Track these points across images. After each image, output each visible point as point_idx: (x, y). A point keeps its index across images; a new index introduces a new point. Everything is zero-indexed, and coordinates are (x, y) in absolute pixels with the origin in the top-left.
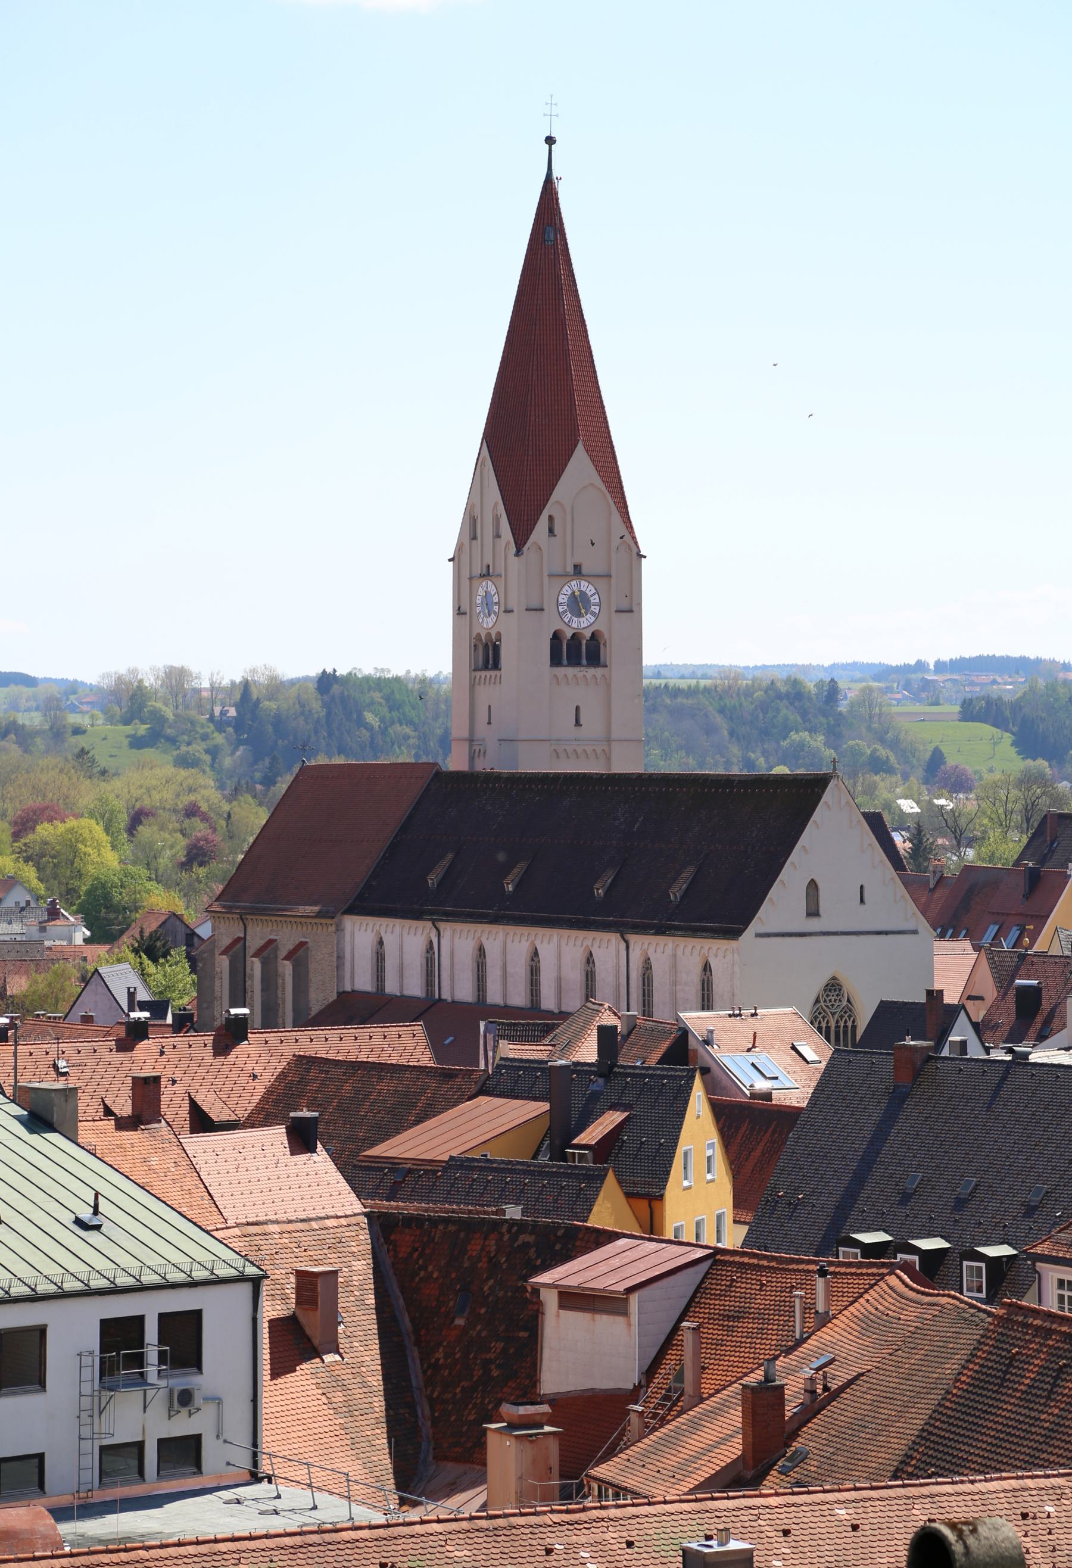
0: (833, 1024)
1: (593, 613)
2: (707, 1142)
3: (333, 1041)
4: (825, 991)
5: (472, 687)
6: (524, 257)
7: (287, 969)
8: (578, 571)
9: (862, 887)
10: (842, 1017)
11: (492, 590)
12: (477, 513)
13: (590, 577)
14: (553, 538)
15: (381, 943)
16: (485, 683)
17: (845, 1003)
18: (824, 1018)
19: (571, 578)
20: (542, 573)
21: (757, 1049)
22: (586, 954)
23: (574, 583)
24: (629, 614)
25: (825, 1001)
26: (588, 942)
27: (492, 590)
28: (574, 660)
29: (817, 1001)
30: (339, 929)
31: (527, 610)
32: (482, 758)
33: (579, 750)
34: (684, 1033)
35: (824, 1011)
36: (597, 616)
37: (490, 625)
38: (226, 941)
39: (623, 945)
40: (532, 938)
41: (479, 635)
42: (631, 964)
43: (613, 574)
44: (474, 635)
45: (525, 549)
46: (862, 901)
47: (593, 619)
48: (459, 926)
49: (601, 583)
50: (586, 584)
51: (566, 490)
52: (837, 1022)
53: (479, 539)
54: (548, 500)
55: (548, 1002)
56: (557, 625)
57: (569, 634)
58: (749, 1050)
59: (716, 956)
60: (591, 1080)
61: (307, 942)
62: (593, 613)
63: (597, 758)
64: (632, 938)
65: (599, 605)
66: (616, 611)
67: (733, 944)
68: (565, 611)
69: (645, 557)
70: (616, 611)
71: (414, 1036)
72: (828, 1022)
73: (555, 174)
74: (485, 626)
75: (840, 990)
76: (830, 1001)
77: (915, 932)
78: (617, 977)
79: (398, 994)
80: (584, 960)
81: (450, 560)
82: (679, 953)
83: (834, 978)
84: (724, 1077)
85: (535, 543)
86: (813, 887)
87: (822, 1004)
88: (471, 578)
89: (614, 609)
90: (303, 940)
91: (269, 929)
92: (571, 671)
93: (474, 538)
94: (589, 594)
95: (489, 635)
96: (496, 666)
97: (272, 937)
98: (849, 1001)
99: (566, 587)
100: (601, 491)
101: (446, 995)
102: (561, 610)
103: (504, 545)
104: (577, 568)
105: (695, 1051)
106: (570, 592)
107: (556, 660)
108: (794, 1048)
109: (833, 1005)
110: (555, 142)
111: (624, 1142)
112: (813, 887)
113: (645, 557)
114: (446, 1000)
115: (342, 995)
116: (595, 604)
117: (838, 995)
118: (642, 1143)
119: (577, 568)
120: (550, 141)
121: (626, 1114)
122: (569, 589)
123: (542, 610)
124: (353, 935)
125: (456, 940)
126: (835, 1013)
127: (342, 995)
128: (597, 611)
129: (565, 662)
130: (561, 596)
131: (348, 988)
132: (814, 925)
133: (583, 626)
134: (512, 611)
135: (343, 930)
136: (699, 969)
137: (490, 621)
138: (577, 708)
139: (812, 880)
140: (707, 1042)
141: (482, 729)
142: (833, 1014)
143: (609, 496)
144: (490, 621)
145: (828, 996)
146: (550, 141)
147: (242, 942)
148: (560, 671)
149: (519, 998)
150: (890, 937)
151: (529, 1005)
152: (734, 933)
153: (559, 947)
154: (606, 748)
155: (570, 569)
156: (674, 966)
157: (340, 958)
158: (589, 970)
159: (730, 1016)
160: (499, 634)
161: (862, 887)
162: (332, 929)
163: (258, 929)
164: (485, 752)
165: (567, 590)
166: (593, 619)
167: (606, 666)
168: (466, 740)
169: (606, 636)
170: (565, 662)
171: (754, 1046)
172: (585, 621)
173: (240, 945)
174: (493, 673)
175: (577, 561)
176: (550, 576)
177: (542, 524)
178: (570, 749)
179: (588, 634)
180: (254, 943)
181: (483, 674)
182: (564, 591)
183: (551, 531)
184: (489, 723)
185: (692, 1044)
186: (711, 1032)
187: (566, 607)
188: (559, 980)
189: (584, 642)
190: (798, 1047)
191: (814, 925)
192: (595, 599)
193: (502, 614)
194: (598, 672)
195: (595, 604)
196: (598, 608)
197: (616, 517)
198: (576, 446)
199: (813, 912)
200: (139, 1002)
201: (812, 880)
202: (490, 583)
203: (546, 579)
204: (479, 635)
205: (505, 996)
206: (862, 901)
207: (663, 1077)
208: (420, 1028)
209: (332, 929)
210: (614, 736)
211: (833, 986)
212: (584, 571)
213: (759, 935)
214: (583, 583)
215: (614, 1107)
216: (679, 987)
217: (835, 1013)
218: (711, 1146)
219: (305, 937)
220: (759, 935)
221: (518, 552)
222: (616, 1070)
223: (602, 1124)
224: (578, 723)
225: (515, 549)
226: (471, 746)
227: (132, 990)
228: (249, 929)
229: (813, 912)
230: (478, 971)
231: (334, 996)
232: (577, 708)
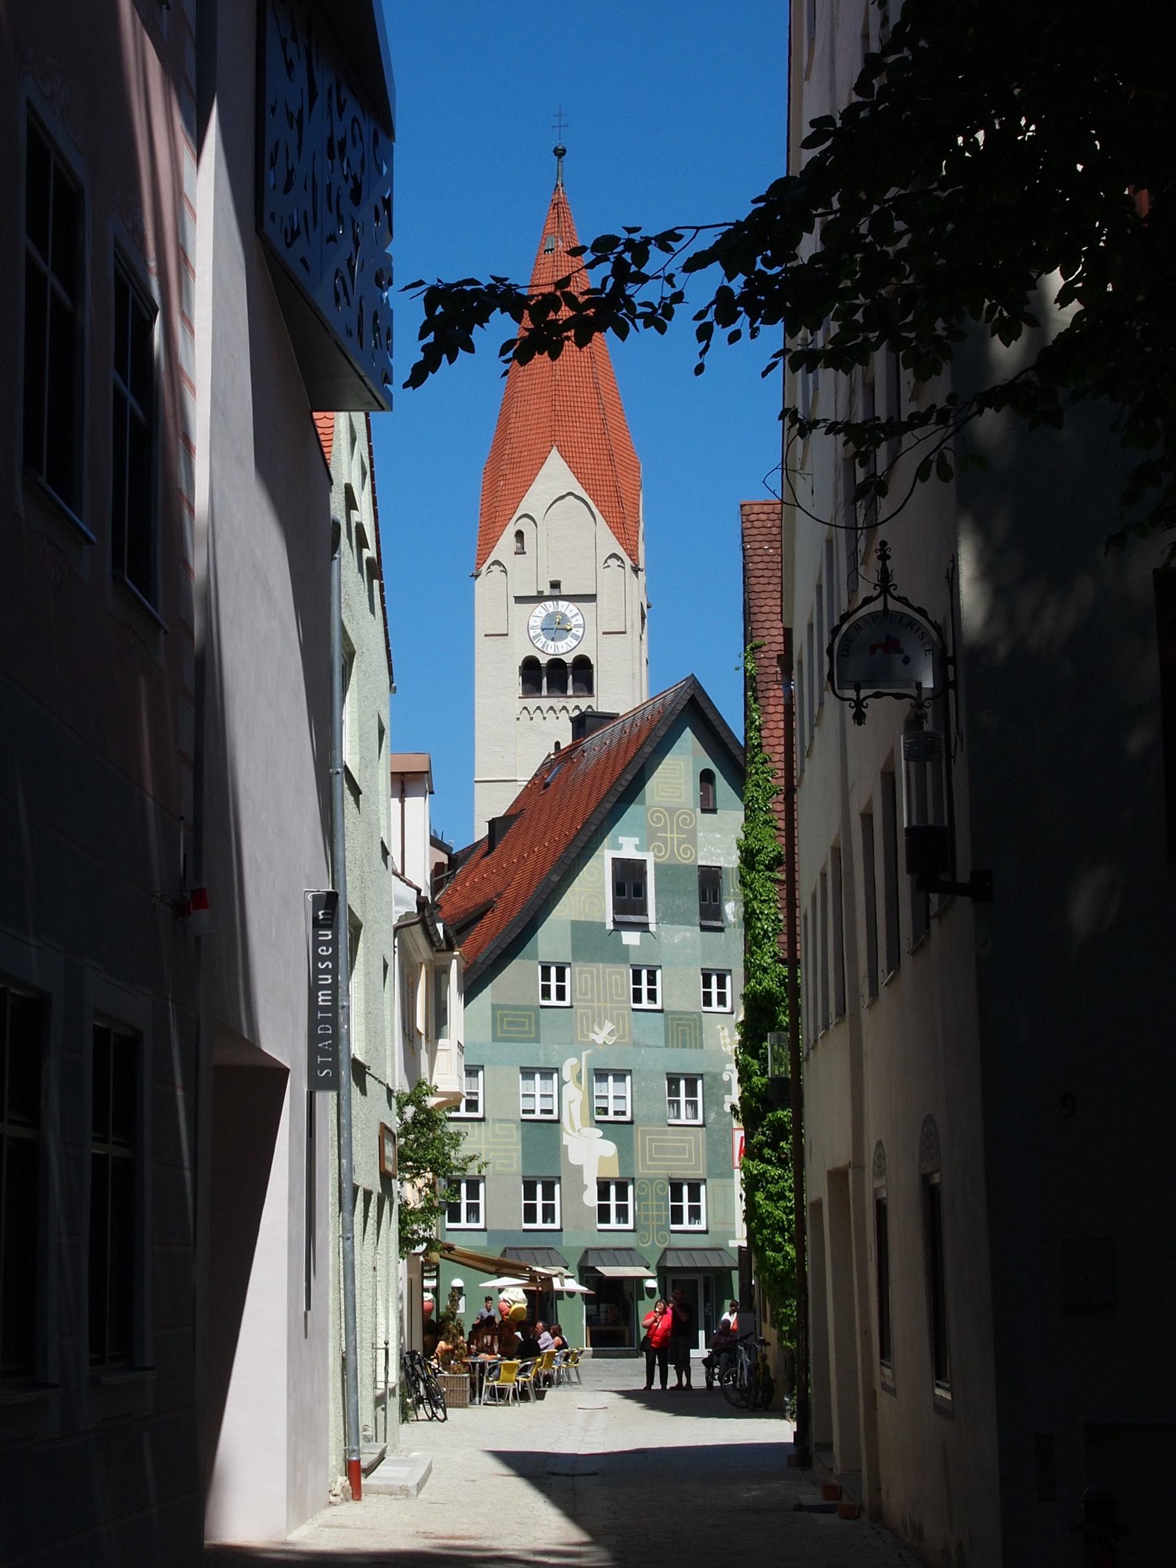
1: (575, 637)
3: (372, 1221)
36: (580, 640)
47: (576, 643)
57: (544, 660)
62: (575, 637)
68: (539, 635)
85: (497, 563)
89: (600, 632)
94: (569, 615)
120: (560, 153)
130: (532, 619)
133: (562, 651)
146: (560, 153)
172: (565, 645)
182: (537, 612)
214: (561, 603)
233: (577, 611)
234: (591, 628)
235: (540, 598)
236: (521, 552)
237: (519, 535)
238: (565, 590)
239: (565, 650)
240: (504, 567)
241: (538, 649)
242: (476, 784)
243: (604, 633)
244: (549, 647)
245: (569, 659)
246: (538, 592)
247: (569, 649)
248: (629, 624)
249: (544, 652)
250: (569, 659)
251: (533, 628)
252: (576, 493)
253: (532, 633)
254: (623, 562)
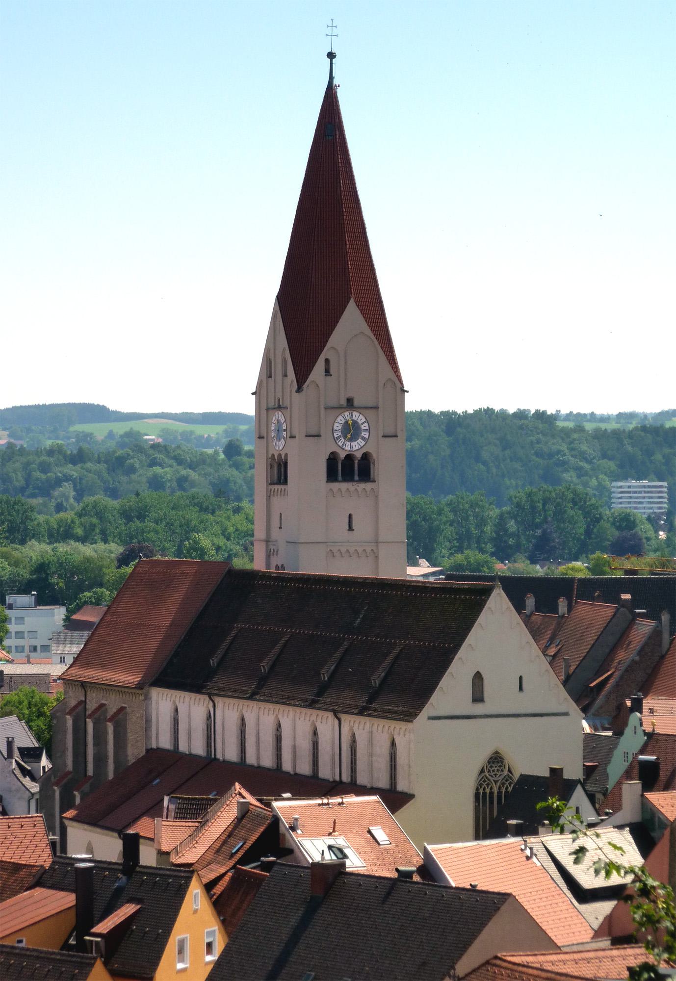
0: (496, 790)
1: (363, 439)
2: (206, 931)
4: (489, 762)
5: (269, 498)
6: (309, 152)
7: (110, 728)
9: (521, 678)
10: (503, 784)
11: (282, 419)
12: (272, 358)
13: (361, 409)
14: (328, 378)
15: (176, 710)
16: (277, 495)
17: (506, 772)
18: (488, 784)
19: (343, 410)
20: (319, 406)
21: (337, 833)
22: (313, 728)
23: (347, 414)
24: (394, 438)
25: (489, 771)
26: (314, 718)
27: (282, 419)
28: (348, 476)
29: (482, 771)
30: (147, 697)
31: (306, 436)
32: (275, 555)
33: (352, 551)
34: (276, 820)
35: (489, 780)
37: (281, 448)
38: (73, 703)
39: (337, 722)
40: (276, 712)
41: (273, 455)
42: (342, 737)
43: (380, 405)
44: (270, 455)
45: (305, 386)
46: (521, 688)
47: (364, 443)
48: (228, 701)
49: (371, 414)
50: (358, 414)
51: (339, 338)
52: (500, 788)
53: (273, 376)
54: (325, 346)
55: (287, 766)
56: (334, 449)
57: (342, 455)
58: (330, 834)
59: (399, 734)
60: (118, 877)
61: (125, 708)
62: (363, 439)
63: (359, 557)
64: (343, 717)
65: (369, 431)
66: (383, 436)
67: (410, 725)
68: (340, 437)
69: (407, 392)
70: (383, 436)
71: (35, 825)
72: (491, 788)
73: (336, 82)
74: (277, 448)
75: (502, 762)
76: (493, 771)
77: (566, 714)
78: (333, 749)
79: (187, 753)
80: (311, 733)
81: (253, 394)
82: (374, 729)
83: (497, 752)
84: (302, 858)
86: (478, 678)
87: (486, 773)
88: (268, 409)
89: (381, 434)
90: (124, 705)
91: (102, 695)
92: (344, 486)
93: (270, 376)
94: (360, 422)
95: (280, 455)
96: (285, 482)
97: (104, 702)
98: (509, 771)
99: (340, 417)
100: (369, 337)
101: (219, 756)
102: (336, 436)
103: (289, 383)
104: (350, 401)
105: (284, 835)
106: (343, 422)
107: (332, 475)
108: (369, 832)
109: (496, 775)
110: (335, 57)
111: (132, 931)
112: (478, 678)
113: (407, 392)
114: (219, 759)
115: (149, 751)
116: (365, 431)
117: (500, 766)
118: (146, 933)
119: (350, 401)
120: (331, 56)
121: (139, 907)
122: (342, 419)
123: (319, 436)
124: (157, 703)
125: (226, 710)
126: (498, 781)
127: (148, 751)
128: (367, 436)
129: (340, 478)
130: (336, 425)
131: (154, 746)
132: (479, 709)
134: (294, 437)
135: (151, 699)
136: (388, 744)
137: (280, 445)
138: (350, 516)
139: (478, 672)
140: (293, 828)
141: (275, 533)
142: (496, 782)
143: (376, 342)
144: (280, 445)
145: (491, 767)
146: (331, 56)
147: (83, 705)
148: (335, 486)
149: (268, 761)
150: (545, 718)
151: (275, 767)
152: (409, 716)
153: (294, 720)
154: (374, 548)
155: (343, 402)
156: (371, 742)
157: (148, 721)
158: (315, 740)
159: (319, 805)
160: (286, 455)
161: (521, 678)
162: (142, 698)
163: (94, 695)
164: (277, 551)
165: (341, 420)
166: (364, 443)
167: (374, 481)
168: (263, 541)
169: (374, 456)
170: (340, 478)
171: (334, 831)
173: (81, 708)
174: (283, 487)
175: (350, 395)
176: (326, 408)
177: (320, 365)
178: (343, 550)
179: (359, 455)
180: (91, 706)
181: (276, 487)
183: (327, 372)
184: (280, 528)
185: (282, 829)
186: (296, 819)
187: (340, 434)
188: (294, 748)
189: (356, 462)
190: (373, 831)
191: (479, 709)
192: (365, 427)
193: (288, 438)
194: (368, 486)
195: (365, 431)
196: (367, 434)
197: (383, 359)
198: (348, 302)
199: (478, 697)
200: (19, 749)
201: (478, 672)
202: (280, 413)
203: (323, 411)
204: (273, 455)
205: (258, 758)
206: (521, 688)
207: (170, 876)
208: (41, 819)
209: (142, 698)
210: (380, 539)
211: (496, 758)
212: (356, 403)
213: (430, 718)
214: (355, 413)
215: (130, 901)
216: (374, 759)
217: (498, 781)
218: (210, 934)
219: (125, 704)
220: (430, 718)
221: (299, 389)
222: (138, 869)
223: (116, 916)
224: (350, 528)
225: (297, 387)
226: (267, 546)
227: (10, 739)
228: (88, 693)
229: (478, 697)
230: (242, 737)
231: (143, 753)
232: (350, 516)
237: (327, 361)
239: (357, 448)
241: (340, 446)
247: (360, 447)
249: (343, 449)
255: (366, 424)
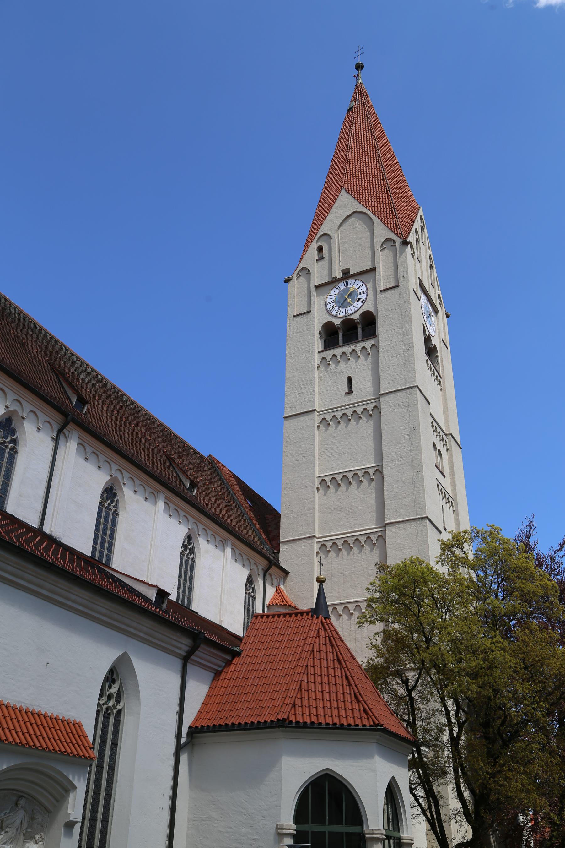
1: (360, 300)
8: (347, 275)
47: (361, 304)
62: (360, 300)
68: (334, 306)
85: (304, 268)
116: (361, 293)
133: (350, 312)
148: (328, 354)
166: (361, 304)
182: (332, 293)
194: (368, 344)
195: (361, 293)
203: (313, 290)
224: (350, 392)
233: (362, 283)
234: (371, 292)
235: (334, 281)
236: (321, 258)
237: (320, 249)
238: (351, 273)
239: (353, 311)
240: (309, 270)
242: (287, 423)
243: (382, 291)
244: (341, 312)
245: (356, 317)
246: (333, 278)
247: (356, 309)
248: (401, 279)
250: (356, 317)
251: (329, 303)
252: (358, 210)
253: (329, 307)
254: (394, 242)
255: (364, 286)
